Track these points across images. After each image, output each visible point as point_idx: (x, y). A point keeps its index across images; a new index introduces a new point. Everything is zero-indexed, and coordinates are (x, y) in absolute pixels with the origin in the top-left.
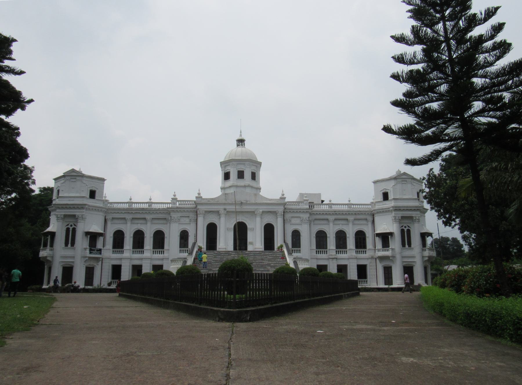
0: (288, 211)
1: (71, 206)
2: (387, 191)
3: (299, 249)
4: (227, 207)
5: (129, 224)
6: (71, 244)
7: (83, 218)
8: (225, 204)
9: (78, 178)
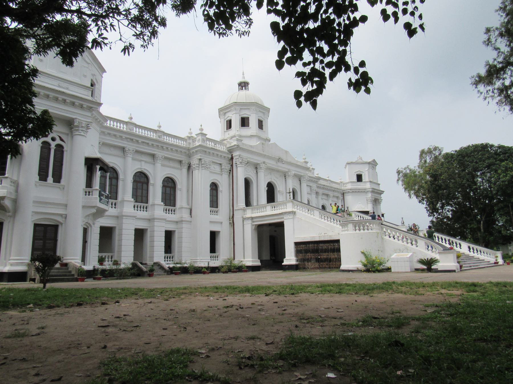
1: (69, 100)
2: (361, 173)
4: (267, 161)
5: (129, 159)
6: (53, 176)
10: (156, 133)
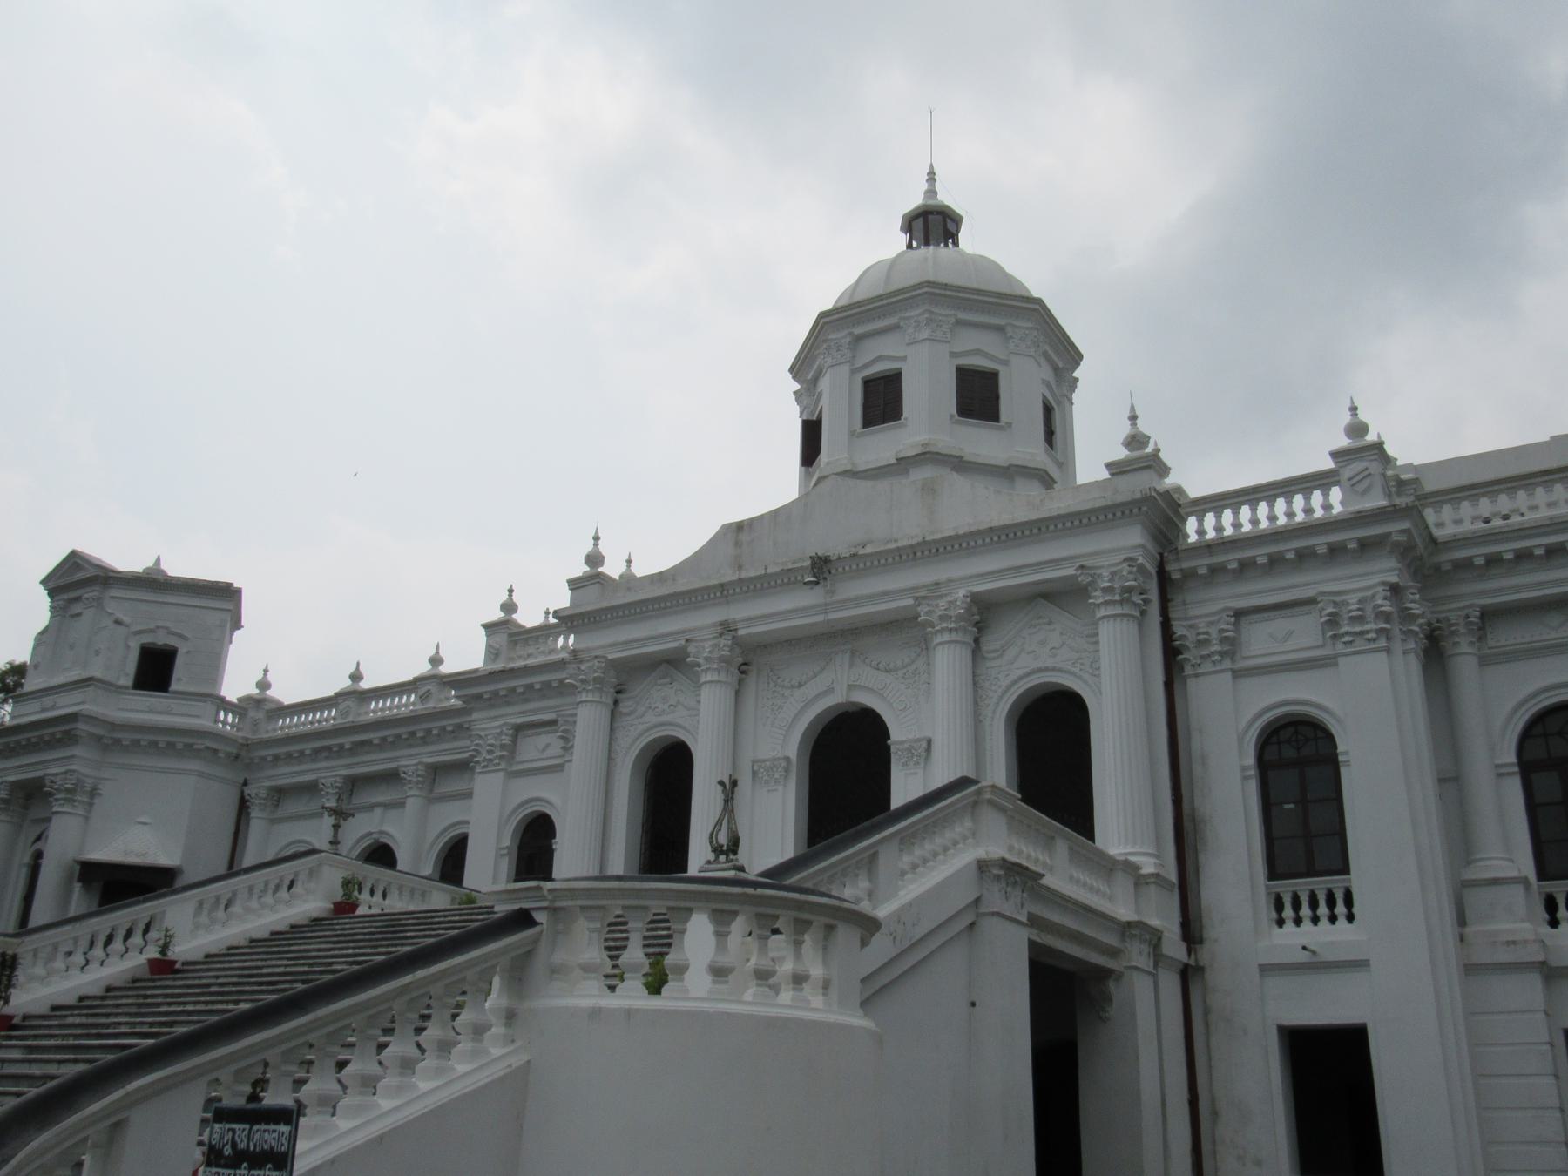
0: (1202, 564)
3: (1336, 883)
7: (86, 794)
8: (722, 592)
9: (88, 593)
10: (415, 690)
